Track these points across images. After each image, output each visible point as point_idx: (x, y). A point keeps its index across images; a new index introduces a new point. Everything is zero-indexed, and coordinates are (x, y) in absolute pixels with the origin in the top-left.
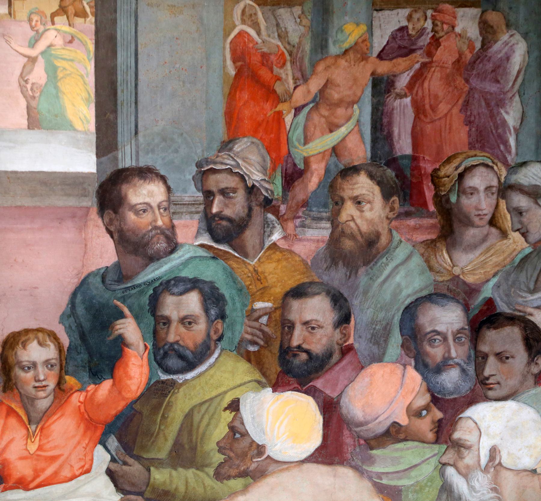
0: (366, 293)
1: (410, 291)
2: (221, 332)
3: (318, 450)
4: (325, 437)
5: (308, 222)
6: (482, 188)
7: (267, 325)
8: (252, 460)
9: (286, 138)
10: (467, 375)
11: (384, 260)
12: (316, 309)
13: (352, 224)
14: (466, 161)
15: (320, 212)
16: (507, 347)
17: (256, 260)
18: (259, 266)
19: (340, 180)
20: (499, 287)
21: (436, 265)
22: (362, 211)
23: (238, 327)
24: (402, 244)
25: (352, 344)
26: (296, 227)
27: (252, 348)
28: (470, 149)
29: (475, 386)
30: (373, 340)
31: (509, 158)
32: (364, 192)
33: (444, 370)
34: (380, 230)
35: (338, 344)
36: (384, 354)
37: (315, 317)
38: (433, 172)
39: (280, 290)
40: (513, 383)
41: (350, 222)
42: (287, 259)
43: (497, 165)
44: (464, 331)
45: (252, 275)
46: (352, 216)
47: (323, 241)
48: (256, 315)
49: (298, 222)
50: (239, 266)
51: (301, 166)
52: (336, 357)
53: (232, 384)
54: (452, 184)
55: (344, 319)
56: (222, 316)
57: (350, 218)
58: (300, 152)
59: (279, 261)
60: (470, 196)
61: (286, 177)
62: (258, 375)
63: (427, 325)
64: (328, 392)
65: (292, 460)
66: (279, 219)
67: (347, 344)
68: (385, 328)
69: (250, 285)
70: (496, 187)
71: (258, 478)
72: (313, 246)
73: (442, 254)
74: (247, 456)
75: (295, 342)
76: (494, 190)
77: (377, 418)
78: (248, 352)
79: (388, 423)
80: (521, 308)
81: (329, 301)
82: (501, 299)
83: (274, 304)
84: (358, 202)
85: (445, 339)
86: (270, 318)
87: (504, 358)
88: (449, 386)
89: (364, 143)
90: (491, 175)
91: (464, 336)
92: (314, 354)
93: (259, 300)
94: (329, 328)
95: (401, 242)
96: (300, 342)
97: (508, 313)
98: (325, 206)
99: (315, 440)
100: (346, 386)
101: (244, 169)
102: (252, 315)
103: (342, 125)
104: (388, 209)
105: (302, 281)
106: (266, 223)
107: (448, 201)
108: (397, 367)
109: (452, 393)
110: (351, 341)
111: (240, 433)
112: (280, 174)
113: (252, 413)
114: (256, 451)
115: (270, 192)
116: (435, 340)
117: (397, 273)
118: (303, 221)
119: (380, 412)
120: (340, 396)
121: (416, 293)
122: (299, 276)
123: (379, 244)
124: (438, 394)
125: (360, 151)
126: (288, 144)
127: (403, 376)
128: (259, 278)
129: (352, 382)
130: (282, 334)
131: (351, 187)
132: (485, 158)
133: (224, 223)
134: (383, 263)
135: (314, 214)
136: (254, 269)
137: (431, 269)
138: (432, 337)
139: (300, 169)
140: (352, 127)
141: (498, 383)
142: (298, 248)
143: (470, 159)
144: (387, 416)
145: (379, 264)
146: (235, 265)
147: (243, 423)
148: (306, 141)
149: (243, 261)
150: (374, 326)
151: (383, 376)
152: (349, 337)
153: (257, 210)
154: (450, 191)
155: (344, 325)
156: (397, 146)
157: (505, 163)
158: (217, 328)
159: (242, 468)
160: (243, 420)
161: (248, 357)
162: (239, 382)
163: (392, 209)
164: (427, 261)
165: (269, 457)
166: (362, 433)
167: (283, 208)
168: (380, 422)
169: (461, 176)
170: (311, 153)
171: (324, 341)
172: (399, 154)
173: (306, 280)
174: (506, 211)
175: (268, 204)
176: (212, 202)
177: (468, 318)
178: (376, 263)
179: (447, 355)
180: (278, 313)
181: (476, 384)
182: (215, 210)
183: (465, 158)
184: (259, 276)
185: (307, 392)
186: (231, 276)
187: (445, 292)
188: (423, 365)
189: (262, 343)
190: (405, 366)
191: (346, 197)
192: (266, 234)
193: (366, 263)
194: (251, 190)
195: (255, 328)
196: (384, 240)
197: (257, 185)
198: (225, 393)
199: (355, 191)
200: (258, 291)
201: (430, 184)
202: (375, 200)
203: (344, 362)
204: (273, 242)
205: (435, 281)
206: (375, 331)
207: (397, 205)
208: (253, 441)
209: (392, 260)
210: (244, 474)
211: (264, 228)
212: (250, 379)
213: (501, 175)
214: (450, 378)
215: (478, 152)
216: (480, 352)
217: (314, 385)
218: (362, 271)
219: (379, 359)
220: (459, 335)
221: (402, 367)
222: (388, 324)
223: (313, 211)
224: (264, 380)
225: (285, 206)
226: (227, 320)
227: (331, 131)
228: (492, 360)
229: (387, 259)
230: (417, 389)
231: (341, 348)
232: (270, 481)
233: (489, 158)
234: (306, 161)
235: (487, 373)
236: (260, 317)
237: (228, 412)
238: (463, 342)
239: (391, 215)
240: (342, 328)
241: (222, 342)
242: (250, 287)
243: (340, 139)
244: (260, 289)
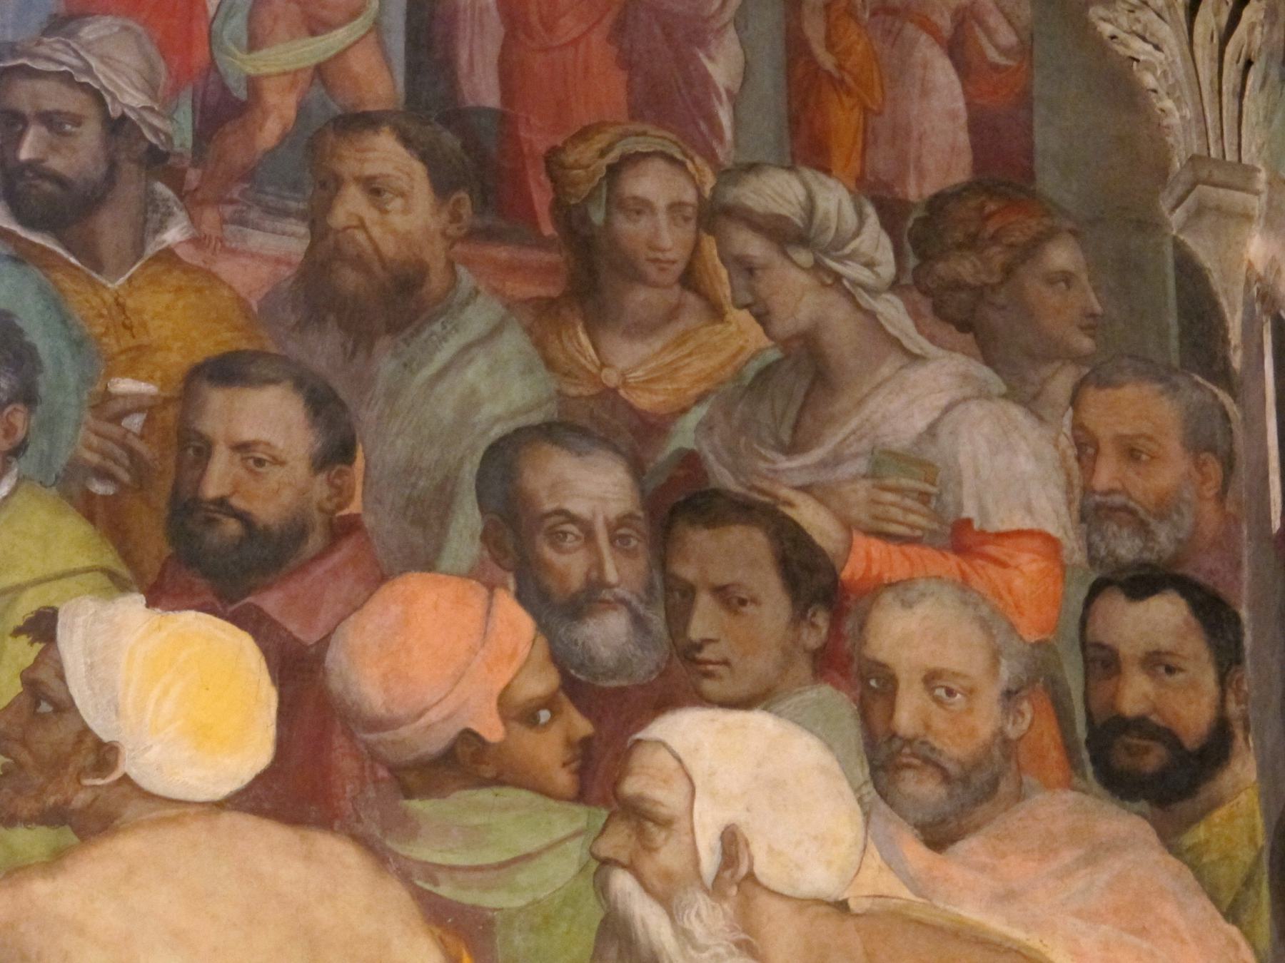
0: (392, 395)
1: (498, 409)
2: (20, 434)
3: (261, 779)
4: (282, 746)
5: (254, 215)
6: (661, 203)
7: (142, 437)
8: (79, 781)
9: (205, 30)
10: (648, 632)
11: (437, 327)
12: (266, 416)
13: (360, 236)
14: (624, 142)
15: (284, 198)
16: (739, 575)
17: (122, 280)
18: (130, 294)
19: (331, 137)
20: (711, 428)
21: (562, 358)
22: (384, 212)
23: (68, 431)
24: (480, 300)
25: (358, 515)
26: (224, 221)
27: (99, 488)
28: (632, 118)
29: (669, 661)
30: (410, 513)
31: (719, 151)
32: (388, 169)
33: (591, 613)
34: (427, 256)
35: (321, 510)
36: (439, 549)
37: (264, 435)
38: (549, 152)
39: (179, 359)
40: (762, 664)
41: (356, 231)
42: (199, 290)
43: (692, 160)
44: (634, 522)
45: (110, 313)
46: (361, 220)
47: (289, 264)
48: (117, 407)
49: (228, 210)
50: (78, 288)
51: (241, 93)
52: (315, 541)
53: (40, 570)
54: (592, 185)
55: (337, 452)
56: (28, 397)
57: (355, 223)
58: (240, 64)
59: (179, 290)
60: (635, 216)
61: (202, 112)
62: (110, 556)
63: (543, 494)
64: (293, 627)
65: (190, 797)
66: (181, 198)
67: (345, 512)
68: (441, 488)
69: (105, 334)
70: (692, 205)
71: (93, 834)
72: (265, 271)
73: (576, 333)
74: (66, 766)
75: (213, 488)
76: (689, 211)
77: (420, 715)
78: (90, 496)
79: (451, 731)
80: (765, 485)
81: (301, 405)
82: (718, 457)
83: (161, 389)
84: (374, 189)
85: (588, 534)
86: (149, 421)
87: (735, 601)
88: (605, 653)
89: (390, 71)
90: (682, 180)
91: (634, 533)
92: (260, 525)
93: (124, 374)
94: (299, 468)
95: (477, 292)
96: (224, 491)
97: (737, 495)
98: (296, 186)
99: (250, 750)
100: (343, 618)
101: (101, 77)
102: (104, 405)
103: (340, 25)
104: (445, 216)
105: (235, 346)
106: (150, 202)
107: (585, 219)
108: (471, 587)
109: (614, 674)
110: (355, 507)
111: (51, 701)
112: (189, 102)
113: (91, 652)
114: (91, 759)
115: (163, 137)
116: (565, 534)
117: (470, 361)
118: (242, 211)
119: (431, 698)
120: (325, 642)
121: (513, 415)
122: (228, 335)
123: (424, 290)
124: (578, 670)
125: (381, 83)
126: (210, 44)
127: (488, 612)
128: (127, 322)
129: (356, 609)
130: (179, 464)
131: (358, 155)
132: (666, 143)
133: (48, 187)
134: (433, 334)
135: (270, 200)
136: (116, 299)
137: (550, 364)
138: (555, 525)
139: (237, 100)
140: (362, 32)
141: (726, 663)
142: (226, 268)
143: (633, 139)
144: (446, 712)
145: (425, 335)
146: (68, 284)
147: (61, 676)
148: (254, 43)
149: (89, 277)
150: (413, 479)
151: (436, 607)
152: (351, 497)
153: (129, 170)
154: (590, 197)
155: (338, 467)
156: (466, 87)
157: (711, 158)
158: (11, 424)
159: (52, 800)
160: (62, 668)
161: (88, 508)
162: (59, 567)
163: (455, 217)
164: (540, 344)
165: (126, 778)
166: (381, 749)
167: (193, 176)
168: (429, 727)
169: (614, 171)
170: (264, 70)
171: (287, 496)
172: (471, 103)
173: (244, 345)
174: (717, 261)
175: (157, 161)
176: (20, 136)
177: (642, 492)
178: (418, 331)
179: (594, 574)
180: (171, 414)
181: (671, 655)
182: (25, 154)
183: (624, 136)
184: (127, 318)
185: (237, 619)
186: (56, 304)
187: (584, 422)
188: (538, 596)
189: (125, 477)
190: (491, 588)
191: (346, 176)
192: (150, 226)
193: (394, 328)
194: (117, 127)
195: (111, 439)
196: (436, 281)
197: (133, 116)
198: (19, 589)
199: (366, 165)
200: (122, 352)
201: (543, 177)
202: (416, 191)
203: (336, 558)
204: (164, 246)
205: (559, 393)
206: (415, 493)
207: (466, 211)
208: (86, 730)
209: (457, 331)
210: (56, 817)
211: (146, 212)
212: (88, 563)
213: (703, 183)
214: (607, 634)
215: (651, 130)
216: (677, 578)
217: (258, 603)
218: (383, 343)
219: (425, 560)
220: (622, 531)
221: (484, 591)
222: (447, 478)
223: (267, 194)
224: (124, 572)
225: (199, 171)
226: (39, 408)
227: (313, 33)
228: (705, 601)
229: (444, 328)
230: (524, 650)
231: (331, 520)
232: (128, 846)
233: (675, 143)
234: (254, 84)
235: (698, 628)
236: (126, 413)
237: (24, 640)
238: (635, 548)
239: (452, 230)
240: (333, 473)
241: (22, 460)
242: (105, 340)
243: (332, 53)
244: (130, 349)
